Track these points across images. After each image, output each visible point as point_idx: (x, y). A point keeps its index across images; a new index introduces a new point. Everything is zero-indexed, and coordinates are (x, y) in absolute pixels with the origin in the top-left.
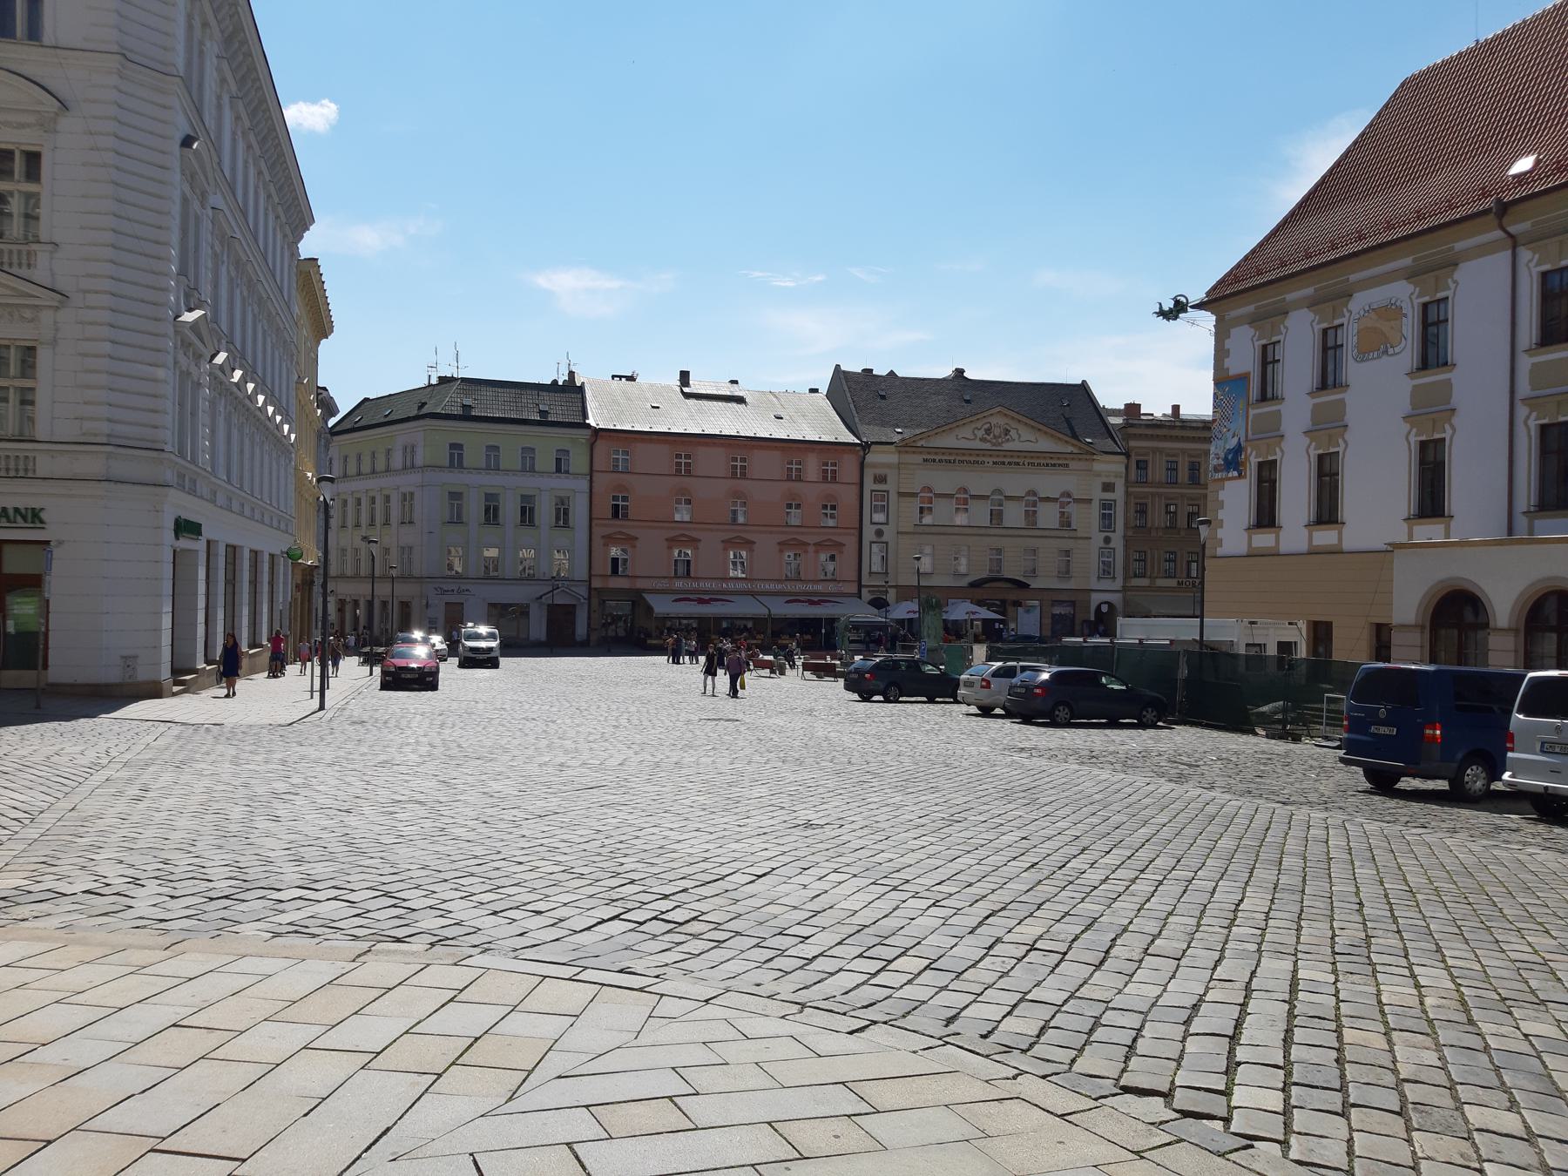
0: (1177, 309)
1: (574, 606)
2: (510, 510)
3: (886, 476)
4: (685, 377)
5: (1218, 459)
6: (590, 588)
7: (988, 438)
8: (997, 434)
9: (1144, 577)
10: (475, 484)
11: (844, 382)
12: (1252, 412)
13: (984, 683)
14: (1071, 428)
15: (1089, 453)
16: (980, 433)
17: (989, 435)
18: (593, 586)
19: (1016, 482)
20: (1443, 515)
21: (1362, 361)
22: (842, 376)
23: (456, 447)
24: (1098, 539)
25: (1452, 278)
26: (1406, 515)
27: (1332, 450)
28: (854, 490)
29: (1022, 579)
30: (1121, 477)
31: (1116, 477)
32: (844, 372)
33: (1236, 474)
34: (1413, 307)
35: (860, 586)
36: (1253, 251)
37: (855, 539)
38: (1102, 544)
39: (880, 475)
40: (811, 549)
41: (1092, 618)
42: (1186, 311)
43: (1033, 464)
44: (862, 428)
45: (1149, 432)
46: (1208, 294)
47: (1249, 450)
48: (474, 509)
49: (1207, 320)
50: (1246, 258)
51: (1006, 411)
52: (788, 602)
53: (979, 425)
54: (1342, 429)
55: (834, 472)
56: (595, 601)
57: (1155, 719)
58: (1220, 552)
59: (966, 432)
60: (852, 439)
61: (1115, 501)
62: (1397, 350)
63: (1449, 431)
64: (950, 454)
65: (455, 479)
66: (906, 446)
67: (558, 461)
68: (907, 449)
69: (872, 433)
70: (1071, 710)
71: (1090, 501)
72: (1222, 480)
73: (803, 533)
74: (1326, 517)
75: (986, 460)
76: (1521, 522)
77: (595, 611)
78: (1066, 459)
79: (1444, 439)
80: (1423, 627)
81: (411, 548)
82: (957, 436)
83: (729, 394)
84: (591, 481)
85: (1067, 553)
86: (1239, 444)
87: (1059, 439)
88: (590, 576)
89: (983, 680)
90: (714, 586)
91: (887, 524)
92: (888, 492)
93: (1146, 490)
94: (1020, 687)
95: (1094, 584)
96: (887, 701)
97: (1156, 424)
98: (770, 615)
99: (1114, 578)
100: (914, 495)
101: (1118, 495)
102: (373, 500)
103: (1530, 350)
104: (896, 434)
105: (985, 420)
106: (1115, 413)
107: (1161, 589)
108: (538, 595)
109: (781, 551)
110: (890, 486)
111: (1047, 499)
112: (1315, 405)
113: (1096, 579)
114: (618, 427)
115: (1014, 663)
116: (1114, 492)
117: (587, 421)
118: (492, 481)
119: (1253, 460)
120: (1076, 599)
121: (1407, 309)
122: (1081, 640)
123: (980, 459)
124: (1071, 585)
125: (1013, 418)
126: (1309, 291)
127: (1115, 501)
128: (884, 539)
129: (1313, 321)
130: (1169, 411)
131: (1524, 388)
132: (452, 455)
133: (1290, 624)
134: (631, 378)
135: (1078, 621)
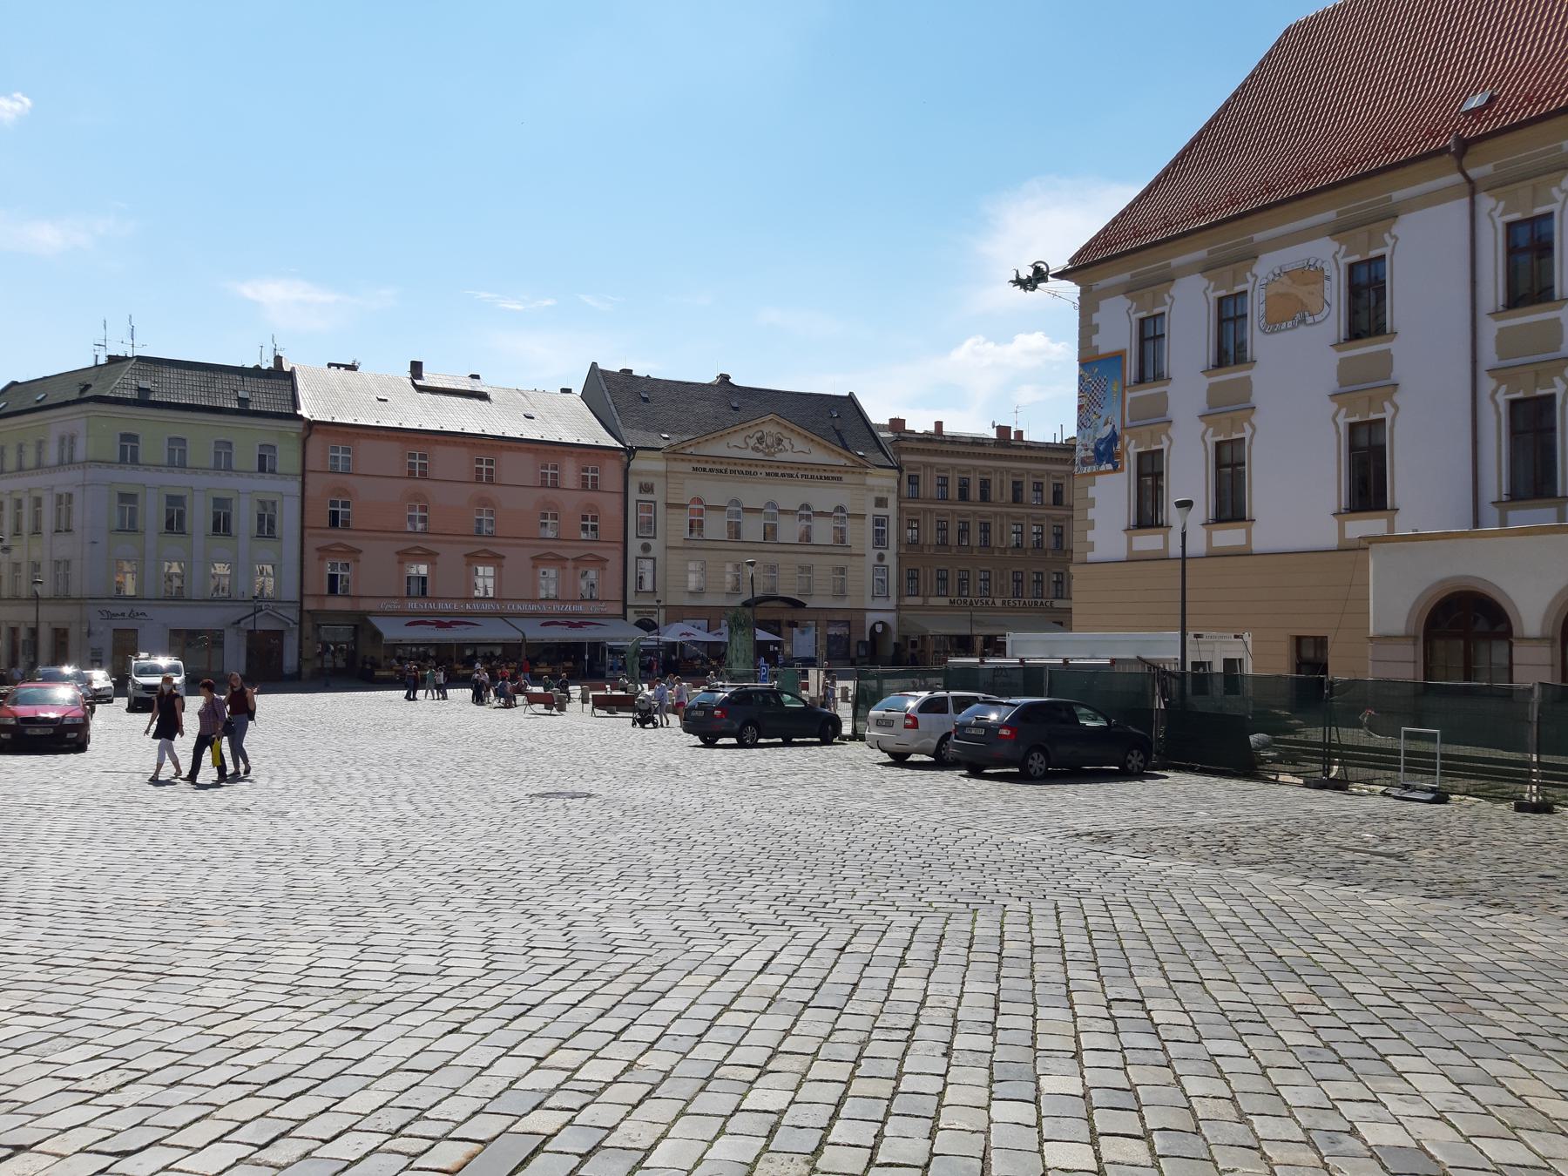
0: (1040, 275)
1: (281, 632)
2: (199, 516)
3: (652, 485)
4: (416, 368)
5: (1087, 450)
6: (301, 611)
8: (769, 444)
9: (917, 595)
10: (153, 485)
11: (602, 381)
12: (1129, 396)
13: (909, 722)
14: (842, 440)
15: (862, 466)
16: (752, 442)
18: (305, 608)
19: (789, 495)
20: (1384, 508)
21: (1273, 332)
22: (599, 375)
23: (129, 438)
24: (872, 555)
25: (1390, 233)
26: (1335, 509)
27: (1235, 436)
28: (618, 499)
29: (796, 598)
31: (888, 491)
32: (602, 370)
33: (1110, 467)
34: (1338, 269)
35: (625, 607)
36: (1122, 214)
38: (876, 562)
40: (570, 564)
41: (867, 639)
42: (1046, 280)
43: (806, 477)
44: (624, 432)
45: (921, 446)
46: (1072, 261)
47: (1127, 438)
48: (152, 513)
49: (1071, 290)
50: (1114, 221)
51: (777, 419)
52: (544, 625)
53: (751, 432)
54: (1250, 411)
55: (595, 479)
56: (308, 626)
57: (1141, 765)
58: (1091, 556)
59: (737, 440)
60: (613, 443)
61: (888, 517)
62: (1318, 318)
63: (1390, 410)
64: (721, 463)
65: (127, 478)
66: (674, 452)
67: (262, 458)
68: (675, 456)
69: (635, 438)
70: (1047, 757)
71: (863, 516)
72: (1093, 474)
73: (561, 547)
74: (1228, 513)
75: (759, 470)
76: (1490, 513)
77: (307, 638)
78: (839, 472)
79: (1383, 420)
80: (1416, 638)
81: (68, 563)
83: (470, 389)
84: (303, 483)
85: (842, 571)
86: (1114, 432)
87: (833, 451)
88: (302, 595)
89: (908, 716)
90: (455, 606)
91: (654, 537)
92: (655, 502)
93: (919, 505)
94: (975, 726)
95: (869, 603)
96: (741, 745)
97: (926, 438)
98: (524, 640)
99: (888, 596)
100: (683, 506)
101: (891, 510)
102: (19, 504)
103: (1497, 312)
104: (662, 440)
105: (757, 428)
106: (882, 427)
107: (934, 608)
108: (238, 618)
109: (535, 567)
110: (658, 496)
111: (822, 514)
112: (1210, 384)
114: (337, 420)
115: (944, 693)
117: (299, 412)
118: (176, 481)
119: (1131, 449)
120: (851, 619)
121: (1330, 270)
122: (977, 660)
123: (753, 469)
124: (846, 604)
125: (786, 427)
126: (1202, 254)
127: (888, 517)
128: (651, 554)
129: (1207, 288)
130: (932, 429)
131: (1489, 356)
132: (123, 448)
133: (1236, 637)
134: (352, 368)
135: (853, 642)
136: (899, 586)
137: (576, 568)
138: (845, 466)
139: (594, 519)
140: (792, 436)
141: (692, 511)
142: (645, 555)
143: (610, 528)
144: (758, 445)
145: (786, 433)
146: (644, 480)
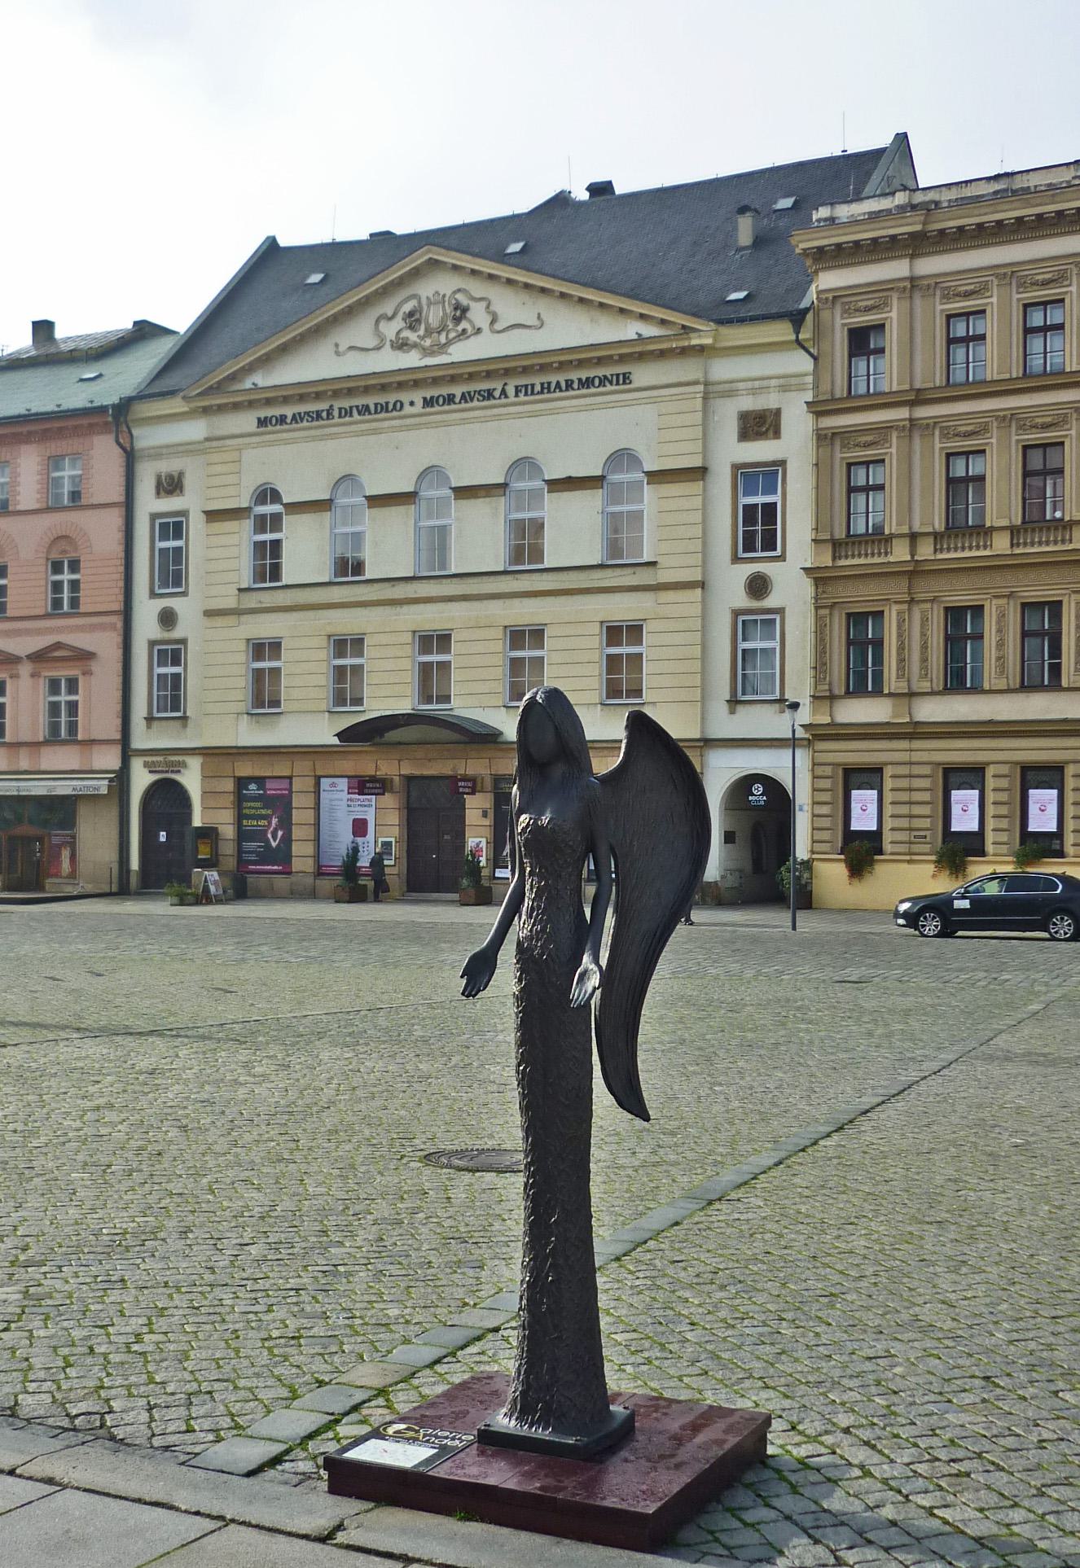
3: (181, 474)
7: (412, 337)
17: (412, 328)
28: (115, 518)
30: (801, 388)
31: (784, 389)
35: (127, 754)
37: (113, 640)
38: (742, 600)
39: (170, 477)
40: (25, 669)
43: (529, 390)
53: (388, 308)
59: (360, 332)
71: (700, 473)
75: (405, 397)
82: (337, 345)
110: (191, 501)
113: (725, 707)
116: (777, 434)
123: (391, 398)
136: (820, 667)
137: (34, 675)
138: (641, 339)
139: (75, 566)
140: (494, 292)
141: (261, 524)
142: (167, 635)
143: (99, 591)
144: (407, 334)
145: (477, 288)
146: (167, 466)
